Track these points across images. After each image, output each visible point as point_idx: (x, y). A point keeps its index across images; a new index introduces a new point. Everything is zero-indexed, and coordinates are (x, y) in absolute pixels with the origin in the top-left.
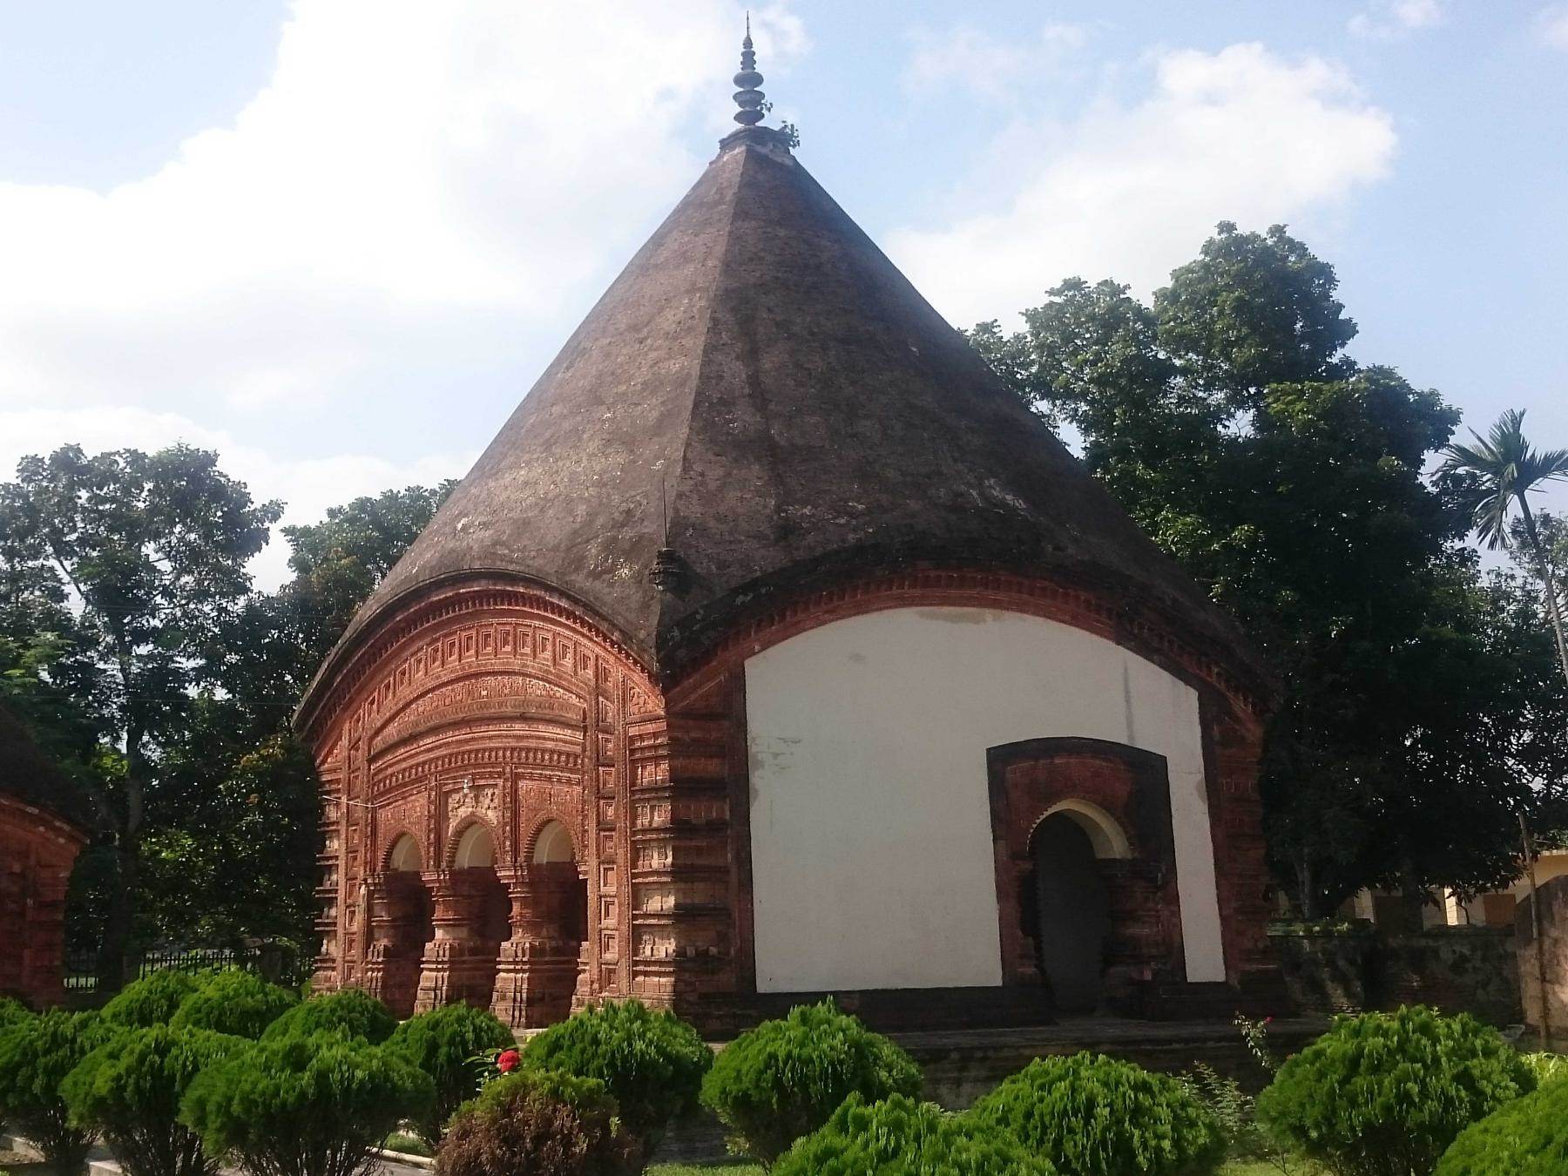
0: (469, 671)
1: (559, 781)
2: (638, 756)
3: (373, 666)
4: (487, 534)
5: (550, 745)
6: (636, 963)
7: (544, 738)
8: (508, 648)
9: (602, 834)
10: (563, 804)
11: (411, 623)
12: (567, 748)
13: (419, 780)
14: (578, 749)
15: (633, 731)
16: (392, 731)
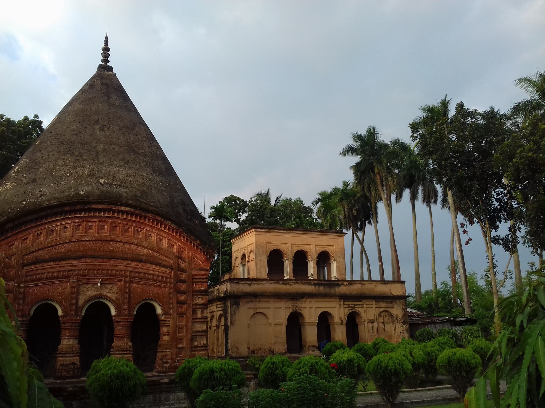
0: (103, 238)
1: (155, 286)
2: (195, 280)
3: (33, 225)
4: (127, 190)
5: (152, 272)
6: (192, 347)
7: (149, 270)
8: (128, 234)
9: (179, 305)
10: (156, 294)
11: (67, 212)
12: (162, 274)
13: (63, 277)
14: (169, 276)
15: (194, 272)
16: (45, 254)
